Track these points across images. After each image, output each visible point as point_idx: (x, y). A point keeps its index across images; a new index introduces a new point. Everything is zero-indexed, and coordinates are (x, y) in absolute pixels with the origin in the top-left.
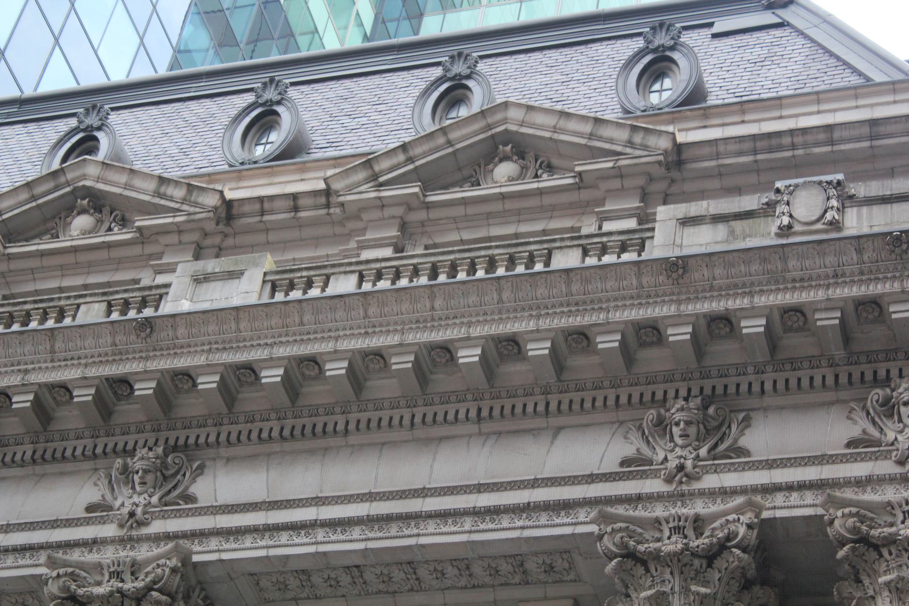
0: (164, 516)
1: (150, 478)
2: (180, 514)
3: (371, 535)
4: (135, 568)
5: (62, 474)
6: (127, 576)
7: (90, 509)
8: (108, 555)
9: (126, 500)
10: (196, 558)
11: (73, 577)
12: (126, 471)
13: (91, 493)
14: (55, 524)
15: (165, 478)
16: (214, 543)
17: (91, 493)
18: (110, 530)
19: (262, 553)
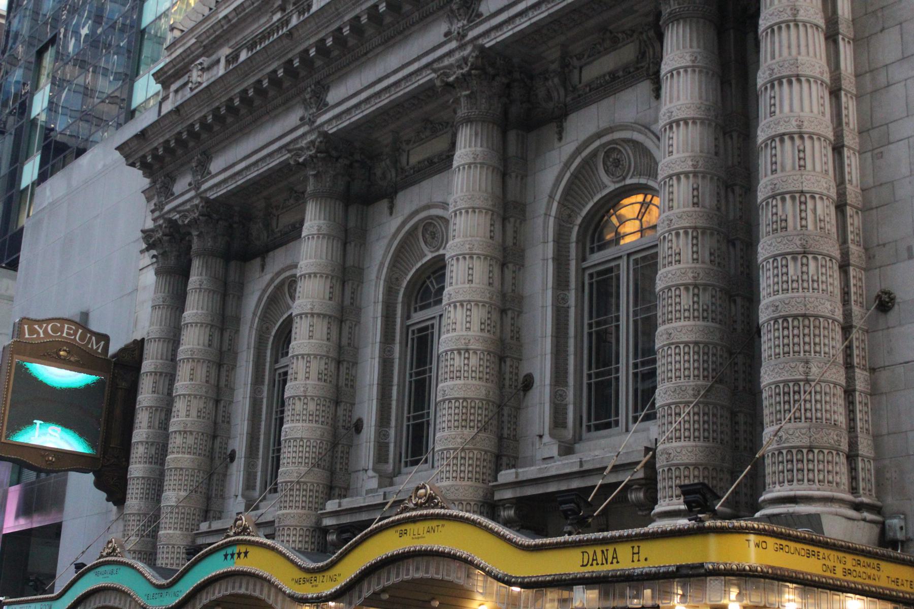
0: (471, 28)
1: (461, 11)
2: (477, 25)
3: (549, 6)
4: (465, 60)
5: (434, 21)
6: (464, 66)
7: (446, 35)
8: (458, 56)
9: (457, 26)
10: (487, 46)
11: (445, 74)
12: (452, 11)
13: (444, 27)
14: (434, 49)
15: (468, 8)
16: (493, 35)
17: (444, 27)
18: (454, 44)
19: (510, 33)
